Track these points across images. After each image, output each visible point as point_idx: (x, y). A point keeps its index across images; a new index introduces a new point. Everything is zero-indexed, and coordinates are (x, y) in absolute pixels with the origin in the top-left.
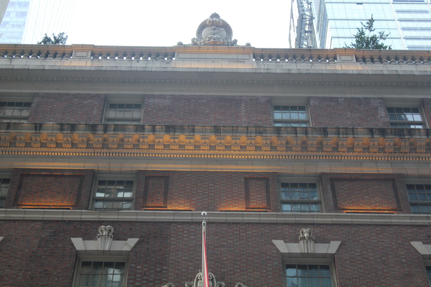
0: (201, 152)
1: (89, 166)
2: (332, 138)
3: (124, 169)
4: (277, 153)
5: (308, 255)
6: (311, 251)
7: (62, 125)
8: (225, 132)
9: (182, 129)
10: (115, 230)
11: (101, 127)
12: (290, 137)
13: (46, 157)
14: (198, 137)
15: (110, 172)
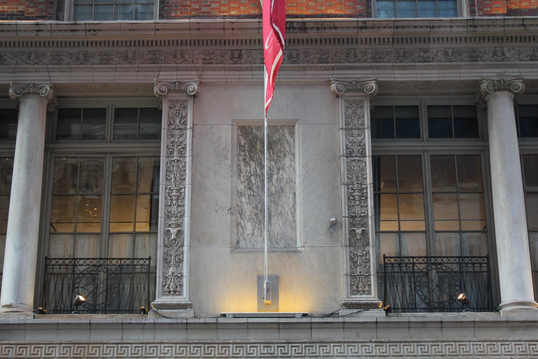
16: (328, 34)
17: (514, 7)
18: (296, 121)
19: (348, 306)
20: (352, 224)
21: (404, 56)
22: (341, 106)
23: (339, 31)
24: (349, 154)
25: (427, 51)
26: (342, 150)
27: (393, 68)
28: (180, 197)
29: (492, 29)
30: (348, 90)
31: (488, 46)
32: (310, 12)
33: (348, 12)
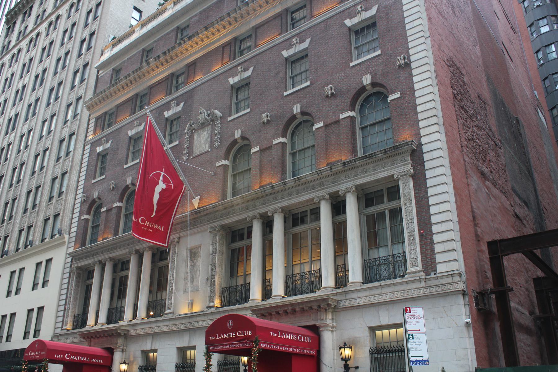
0: (205, 42)
1: (170, 72)
2: (162, 59)
3: (181, 67)
4: (233, 26)
5: (362, 21)
6: (242, 78)
7: (155, 58)
8: (210, 28)
9: (193, 36)
10: (177, 101)
11: (167, 52)
12: (234, 15)
13: (157, 74)
14: (200, 35)
15: (178, 70)
16: (206, 212)
17: (262, 184)
18: (201, 245)
19: (207, 307)
20: (212, 279)
21: (228, 214)
22: (212, 235)
23: (209, 210)
24: (213, 254)
25: (234, 210)
26: (211, 253)
27: (225, 219)
28: (173, 277)
29: (248, 198)
30: (213, 230)
31: (251, 203)
32: (207, 204)
33: (217, 201)
